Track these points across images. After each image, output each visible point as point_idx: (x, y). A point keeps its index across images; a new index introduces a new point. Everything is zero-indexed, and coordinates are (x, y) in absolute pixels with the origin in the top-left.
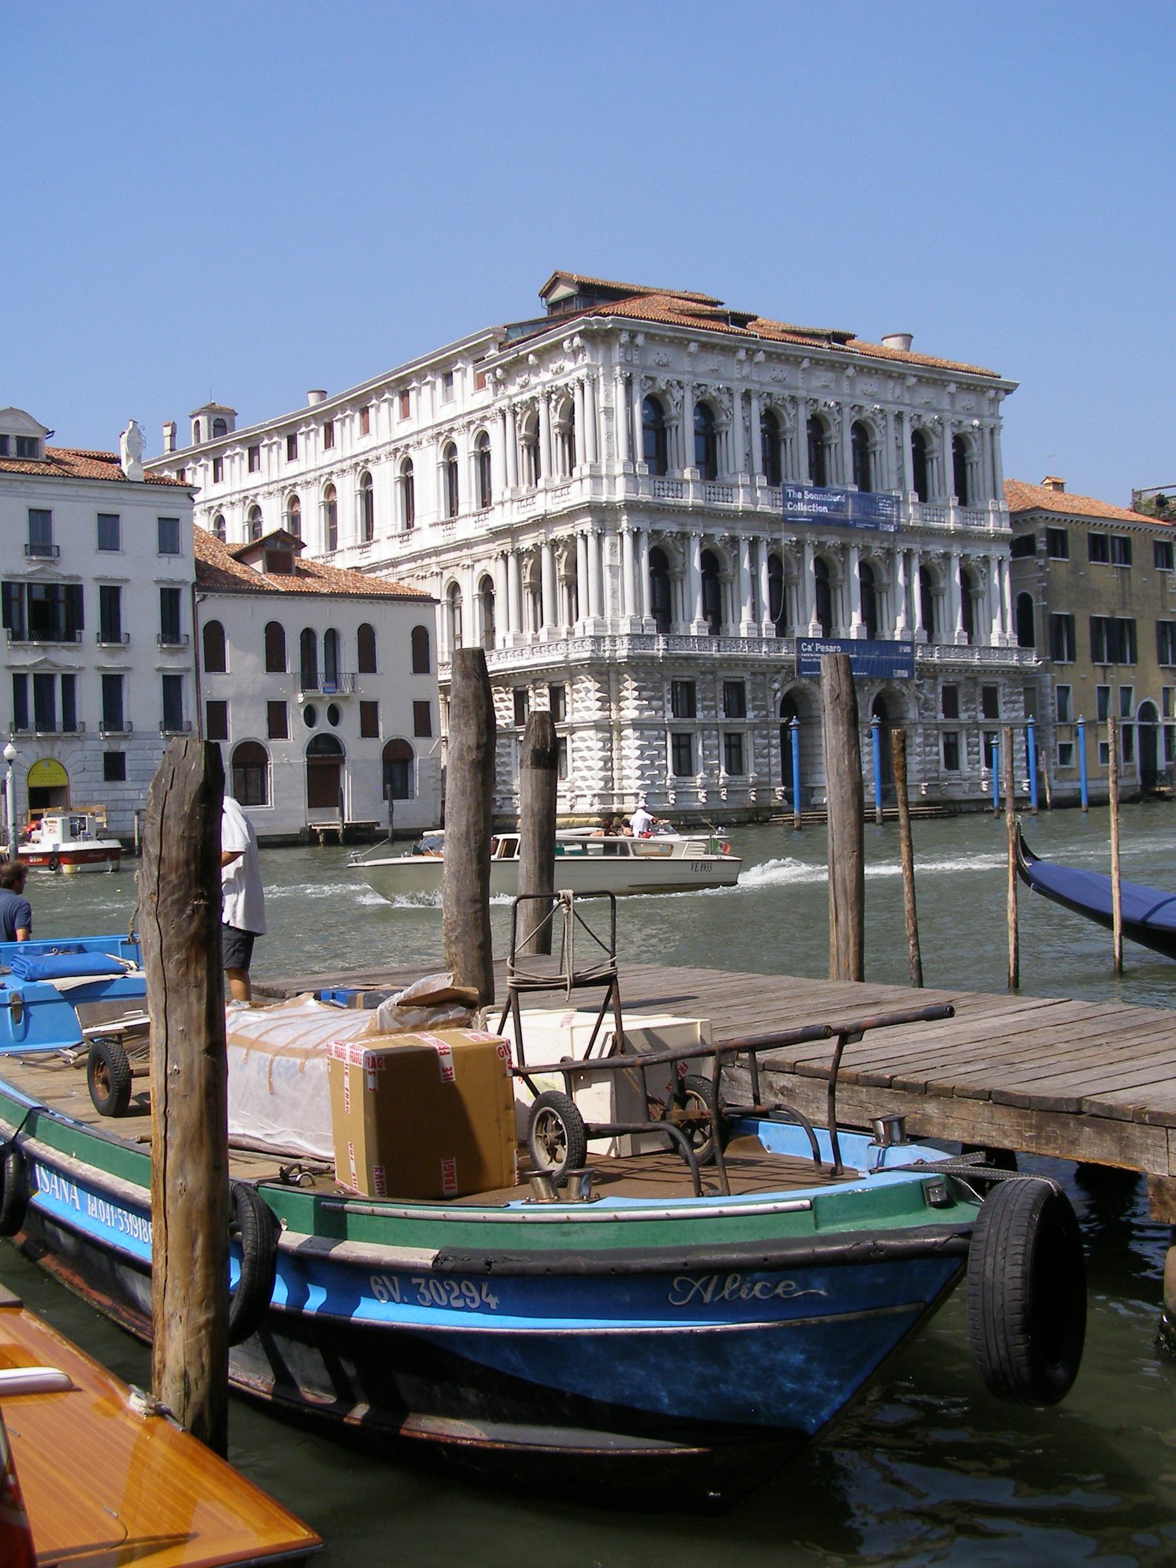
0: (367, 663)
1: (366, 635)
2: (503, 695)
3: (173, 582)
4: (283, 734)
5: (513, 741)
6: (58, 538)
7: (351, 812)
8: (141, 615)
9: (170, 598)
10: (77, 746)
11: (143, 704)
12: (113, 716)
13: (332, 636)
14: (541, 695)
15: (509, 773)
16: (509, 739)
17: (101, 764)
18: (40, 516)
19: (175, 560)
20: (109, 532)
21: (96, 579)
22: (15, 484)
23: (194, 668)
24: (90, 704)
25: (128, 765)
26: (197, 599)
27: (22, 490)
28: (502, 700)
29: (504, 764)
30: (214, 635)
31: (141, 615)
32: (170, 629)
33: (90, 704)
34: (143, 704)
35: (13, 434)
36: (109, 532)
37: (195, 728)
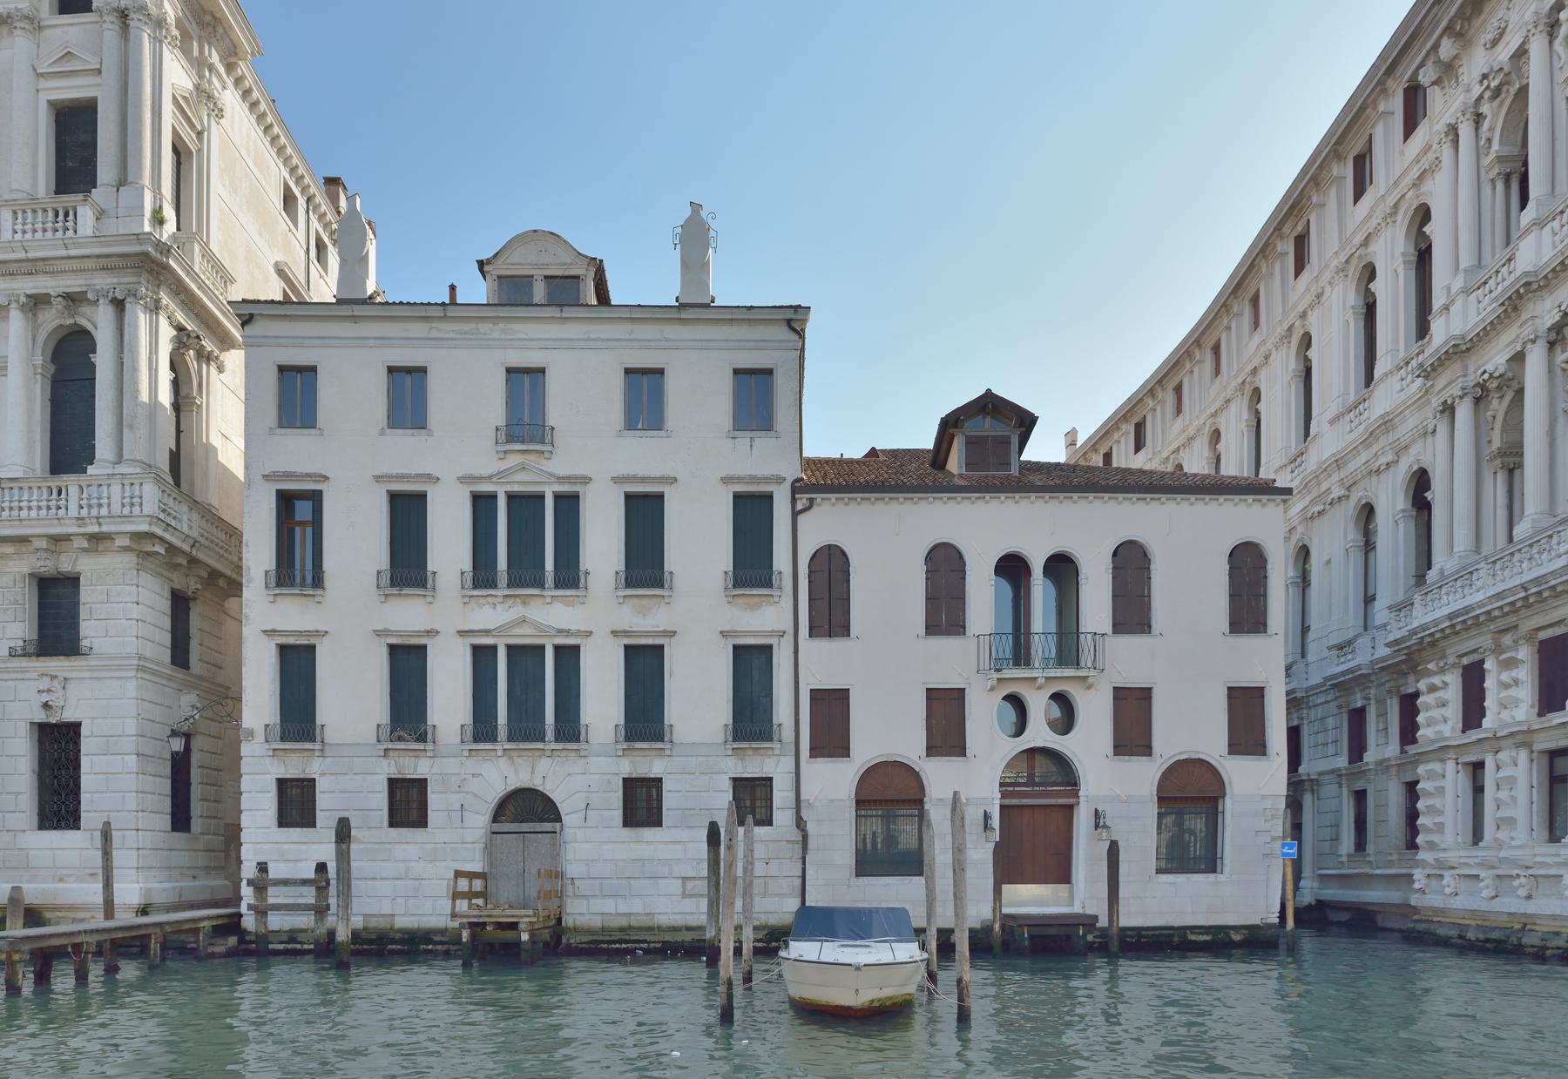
0: (1132, 612)
1: (1131, 564)
2: (1436, 680)
3: (753, 479)
4: (960, 749)
5: (1450, 765)
6: (555, 415)
7: (1081, 896)
8: (699, 541)
9: (751, 512)
10: (575, 765)
11: (698, 696)
12: (645, 716)
13: (1062, 567)
14: (1511, 663)
15: (1440, 827)
16: (1443, 761)
17: (617, 797)
18: (526, 378)
19: (764, 442)
20: (644, 396)
21: (617, 480)
22: (484, 327)
23: (791, 631)
24: (603, 697)
25: (668, 801)
26: (799, 507)
27: (496, 335)
28: (1433, 689)
29: (1432, 810)
30: (831, 569)
31: (699, 541)
32: (751, 565)
33: (603, 697)
34: (698, 696)
35: (539, 273)
36: (644, 396)
37: (787, 734)
